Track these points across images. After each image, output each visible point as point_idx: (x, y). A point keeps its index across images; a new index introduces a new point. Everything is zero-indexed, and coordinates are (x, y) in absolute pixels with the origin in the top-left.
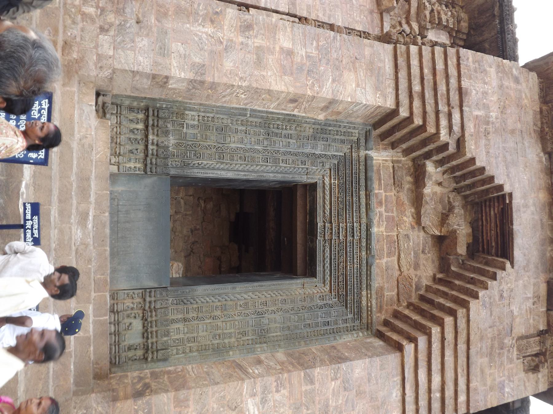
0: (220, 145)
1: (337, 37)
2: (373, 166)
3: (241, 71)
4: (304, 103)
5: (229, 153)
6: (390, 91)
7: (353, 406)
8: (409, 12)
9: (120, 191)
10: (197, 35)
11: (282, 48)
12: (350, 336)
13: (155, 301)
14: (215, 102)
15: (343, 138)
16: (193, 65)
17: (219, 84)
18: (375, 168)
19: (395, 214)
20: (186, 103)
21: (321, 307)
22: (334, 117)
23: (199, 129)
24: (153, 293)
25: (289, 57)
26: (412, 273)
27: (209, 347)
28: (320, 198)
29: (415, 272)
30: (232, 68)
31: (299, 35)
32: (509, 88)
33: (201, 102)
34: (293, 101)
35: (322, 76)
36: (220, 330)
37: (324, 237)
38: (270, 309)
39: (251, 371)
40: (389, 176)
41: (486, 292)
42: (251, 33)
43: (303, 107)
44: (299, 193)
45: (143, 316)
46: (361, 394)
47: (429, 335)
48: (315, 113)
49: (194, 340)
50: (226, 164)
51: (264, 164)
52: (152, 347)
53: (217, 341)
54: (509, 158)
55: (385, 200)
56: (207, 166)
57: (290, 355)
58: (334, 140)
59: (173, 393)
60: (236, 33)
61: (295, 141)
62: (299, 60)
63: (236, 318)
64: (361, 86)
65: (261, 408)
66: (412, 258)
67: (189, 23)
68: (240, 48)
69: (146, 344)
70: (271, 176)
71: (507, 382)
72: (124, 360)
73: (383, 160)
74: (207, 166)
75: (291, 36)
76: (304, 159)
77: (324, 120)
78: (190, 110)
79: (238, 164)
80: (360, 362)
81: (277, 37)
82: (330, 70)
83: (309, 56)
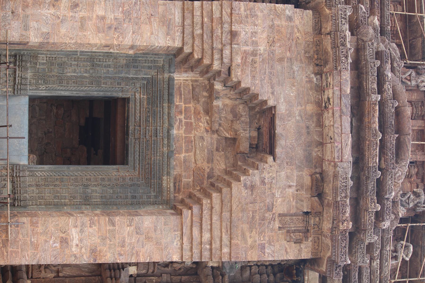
0: (60, 75)
1: (137, 2)
6: (178, 34)
7: (142, 245)
10: (44, 15)
11: (97, 16)
12: (152, 207)
13: (19, 172)
15: (150, 64)
16: (42, 34)
17: (57, 43)
18: (176, 87)
19: (193, 121)
21: (131, 185)
25: (102, 21)
27: (51, 203)
28: (132, 108)
29: (208, 165)
31: (110, 6)
32: (280, 26)
33: (48, 49)
36: (59, 193)
37: (135, 136)
40: (189, 92)
41: (248, 178)
42: (78, 9)
45: (13, 180)
46: (149, 238)
47: (202, 205)
49: (42, 198)
50: (64, 87)
51: (90, 85)
52: (17, 199)
53: (56, 200)
55: (185, 110)
56: (51, 89)
58: (143, 67)
59: (30, 218)
60: (68, 11)
61: (113, 69)
62: (109, 22)
63: (70, 187)
64: (154, 34)
65: (80, 235)
66: (206, 154)
67: (40, 9)
68: (70, 19)
70: (95, 94)
71: (266, 245)
74: (51, 89)
75: (104, 7)
76: (119, 81)
78: (41, 54)
79: (72, 86)
81: (94, 9)
82: (131, 25)
83: (116, 19)
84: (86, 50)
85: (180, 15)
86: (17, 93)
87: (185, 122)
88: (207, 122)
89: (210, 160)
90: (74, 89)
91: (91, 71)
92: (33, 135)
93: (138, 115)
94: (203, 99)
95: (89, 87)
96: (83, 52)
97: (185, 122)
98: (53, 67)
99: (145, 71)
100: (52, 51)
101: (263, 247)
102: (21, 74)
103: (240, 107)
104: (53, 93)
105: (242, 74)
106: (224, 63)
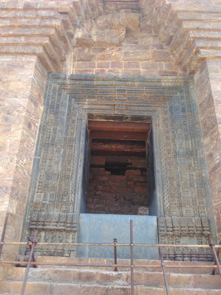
0: (59, 178)
2: (77, 75)
3: (6, 161)
4: (31, 118)
5: (65, 171)
9: (89, 250)
14: (28, 180)
15: (57, 94)
18: (78, 73)
19: (110, 61)
20: (28, 201)
21: (172, 113)
22: (42, 99)
23: (47, 192)
24: (162, 229)
26: (150, 51)
30: (3, 167)
33: (28, 190)
34: (29, 126)
35: (12, 104)
37: (124, 110)
38: (173, 147)
39: (218, 161)
40: (84, 64)
43: (34, 119)
44: (93, 126)
45: (178, 236)
48: (39, 112)
50: (73, 174)
51: (73, 148)
57: (206, 135)
58: (59, 100)
61: (58, 127)
66: (141, 50)
69: (198, 235)
70: (82, 144)
72: (210, 251)
73: (73, 67)
74: (74, 188)
76: (71, 121)
77: (44, 106)
78: (33, 199)
79: (73, 166)
80: (212, 86)
82: (8, 99)
84: (35, 150)
85: (5, 56)
86: (76, 227)
87: (111, 68)
88: (112, 49)
89: (146, 48)
90: (76, 164)
91: (59, 146)
92: (118, 210)
93: (104, 107)
94: (91, 52)
95: (75, 150)
96: (36, 153)
97: (111, 68)
98: (50, 186)
99: (63, 99)
100: (31, 185)
102: (54, 222)
103: (99, 23)
104: (79, 185)
106: (54, 15)
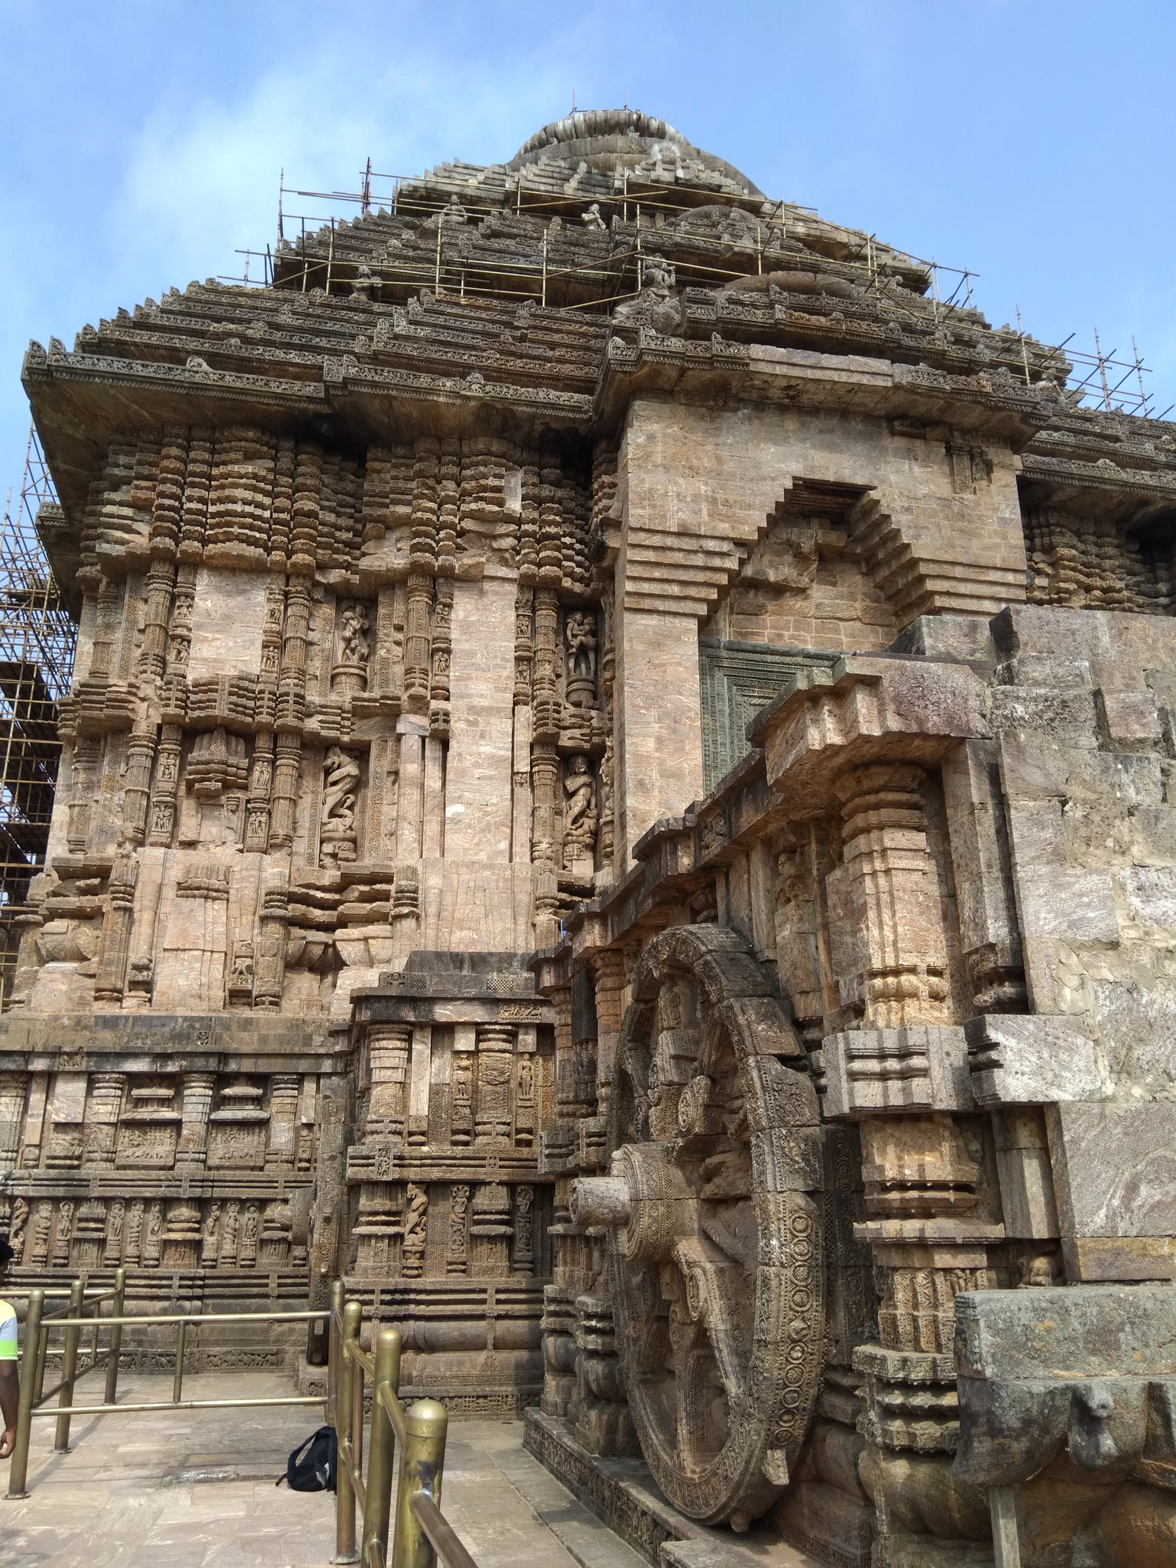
6: (677, 621)
8: (480, 535)
11: (657, 750)
19: (791, 618)
54: (752, 473)
101: (1003, 521)
105: (746, 523)
